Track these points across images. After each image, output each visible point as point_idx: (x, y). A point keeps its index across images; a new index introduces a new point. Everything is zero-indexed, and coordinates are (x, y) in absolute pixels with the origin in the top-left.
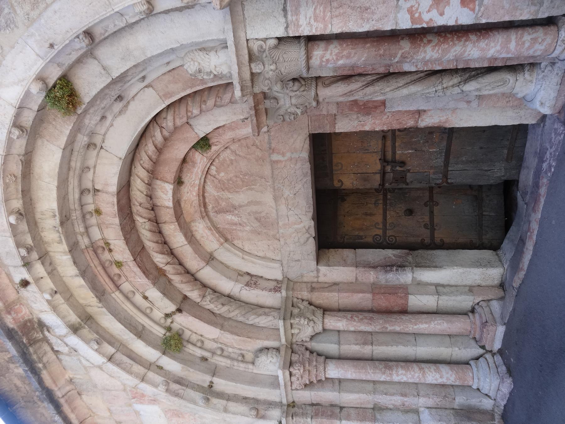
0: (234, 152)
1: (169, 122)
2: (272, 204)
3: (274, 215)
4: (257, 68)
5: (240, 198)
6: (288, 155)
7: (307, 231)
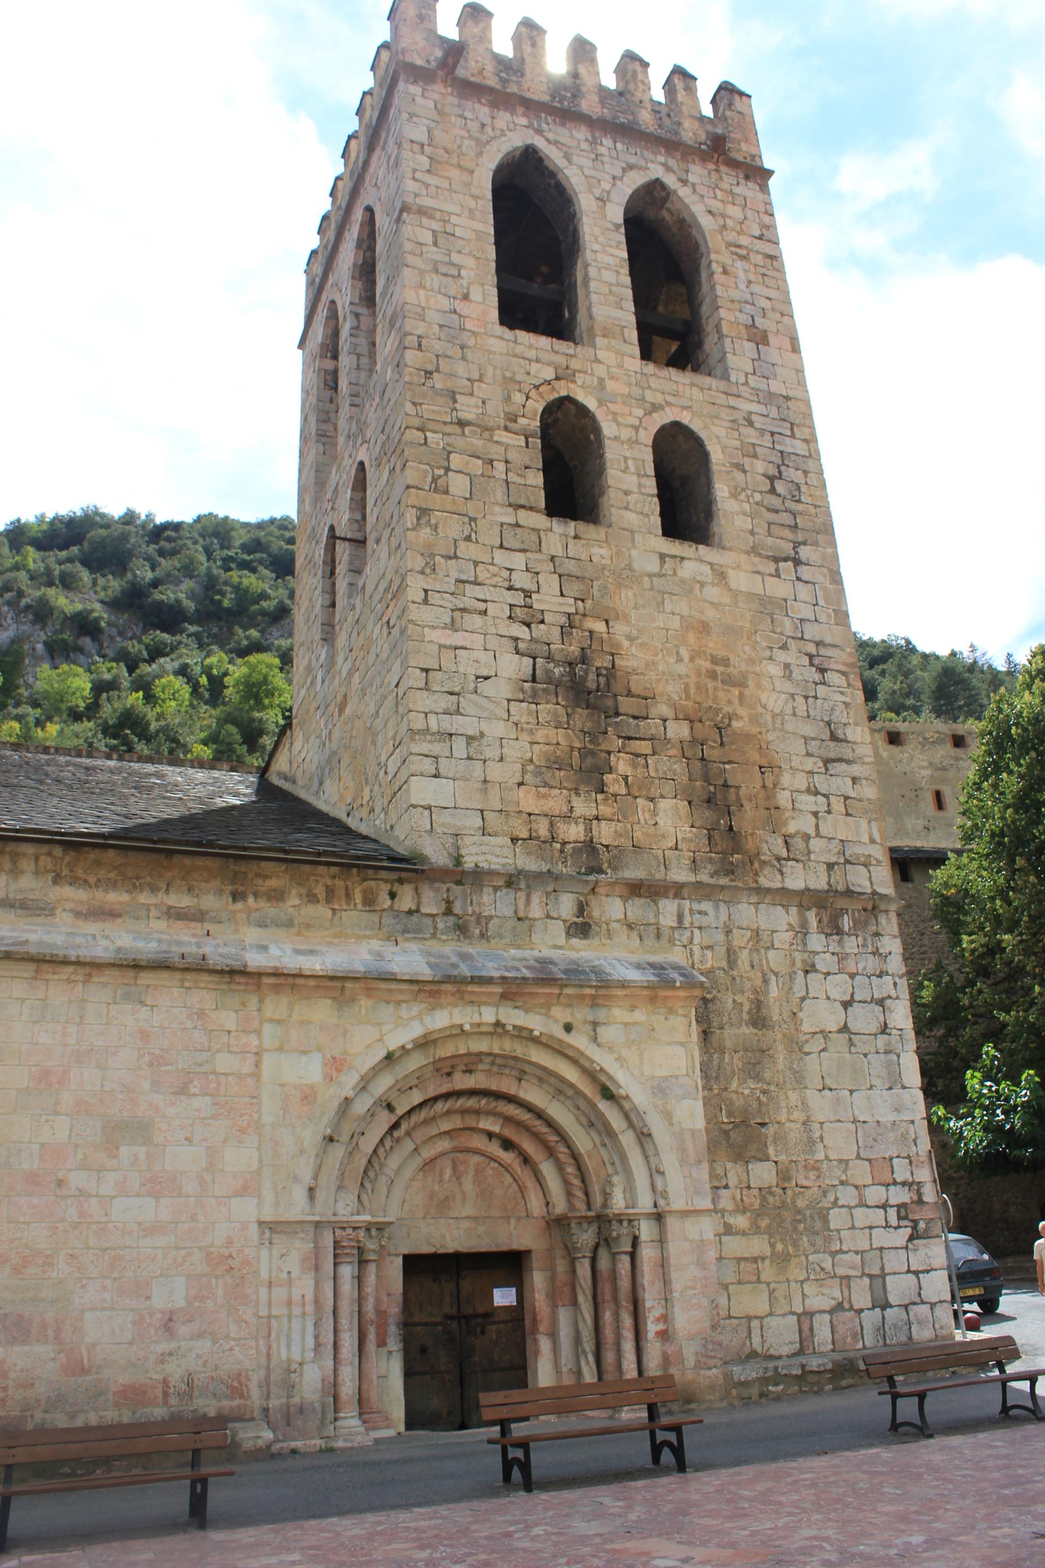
0: (510, 1186)
1: (562, 1148)
2: (463, 1215)
3: (453, 1214)
4: (625, 1223)
5: (468, 1185)
6: (515, 1232)
7: (442, 1246)
